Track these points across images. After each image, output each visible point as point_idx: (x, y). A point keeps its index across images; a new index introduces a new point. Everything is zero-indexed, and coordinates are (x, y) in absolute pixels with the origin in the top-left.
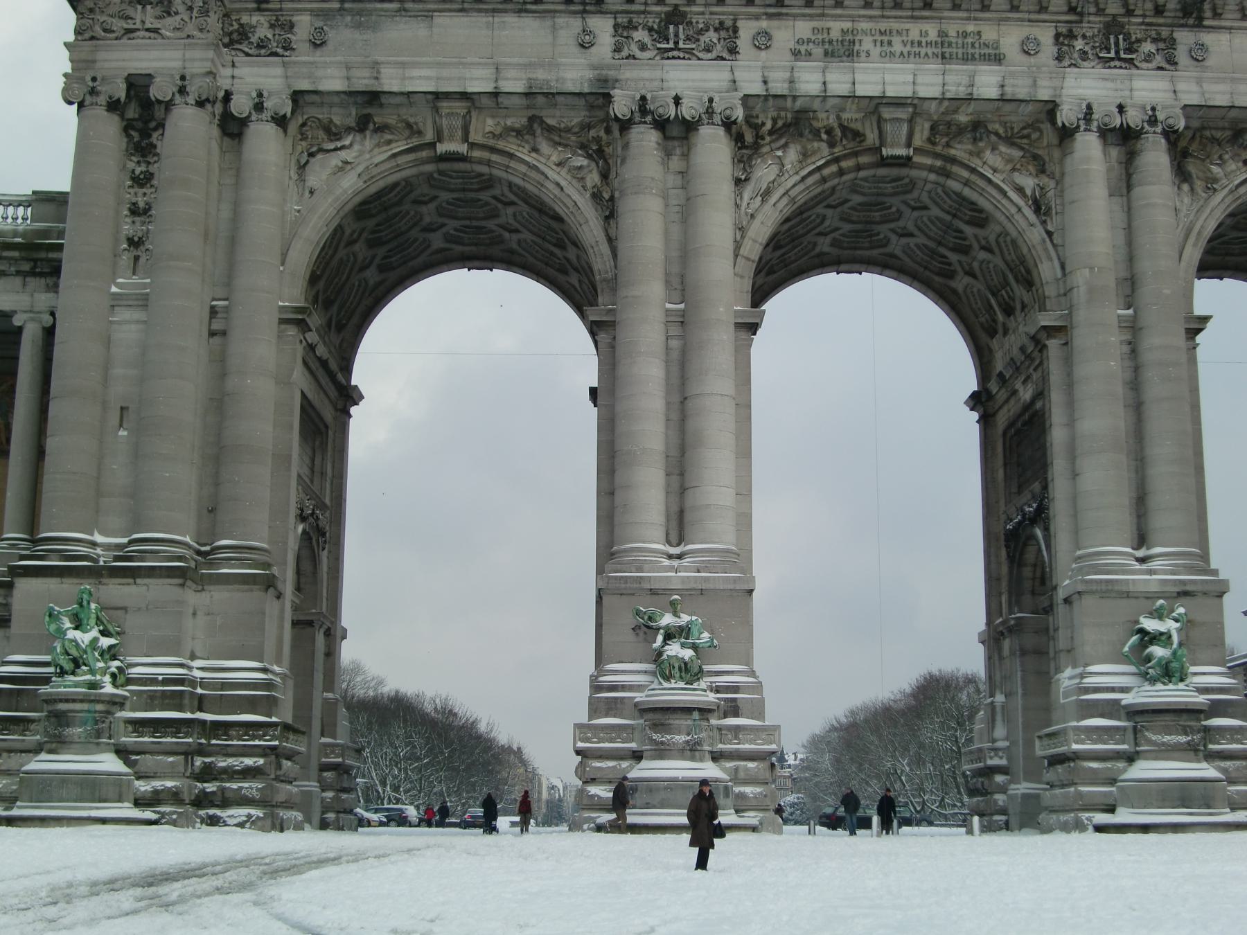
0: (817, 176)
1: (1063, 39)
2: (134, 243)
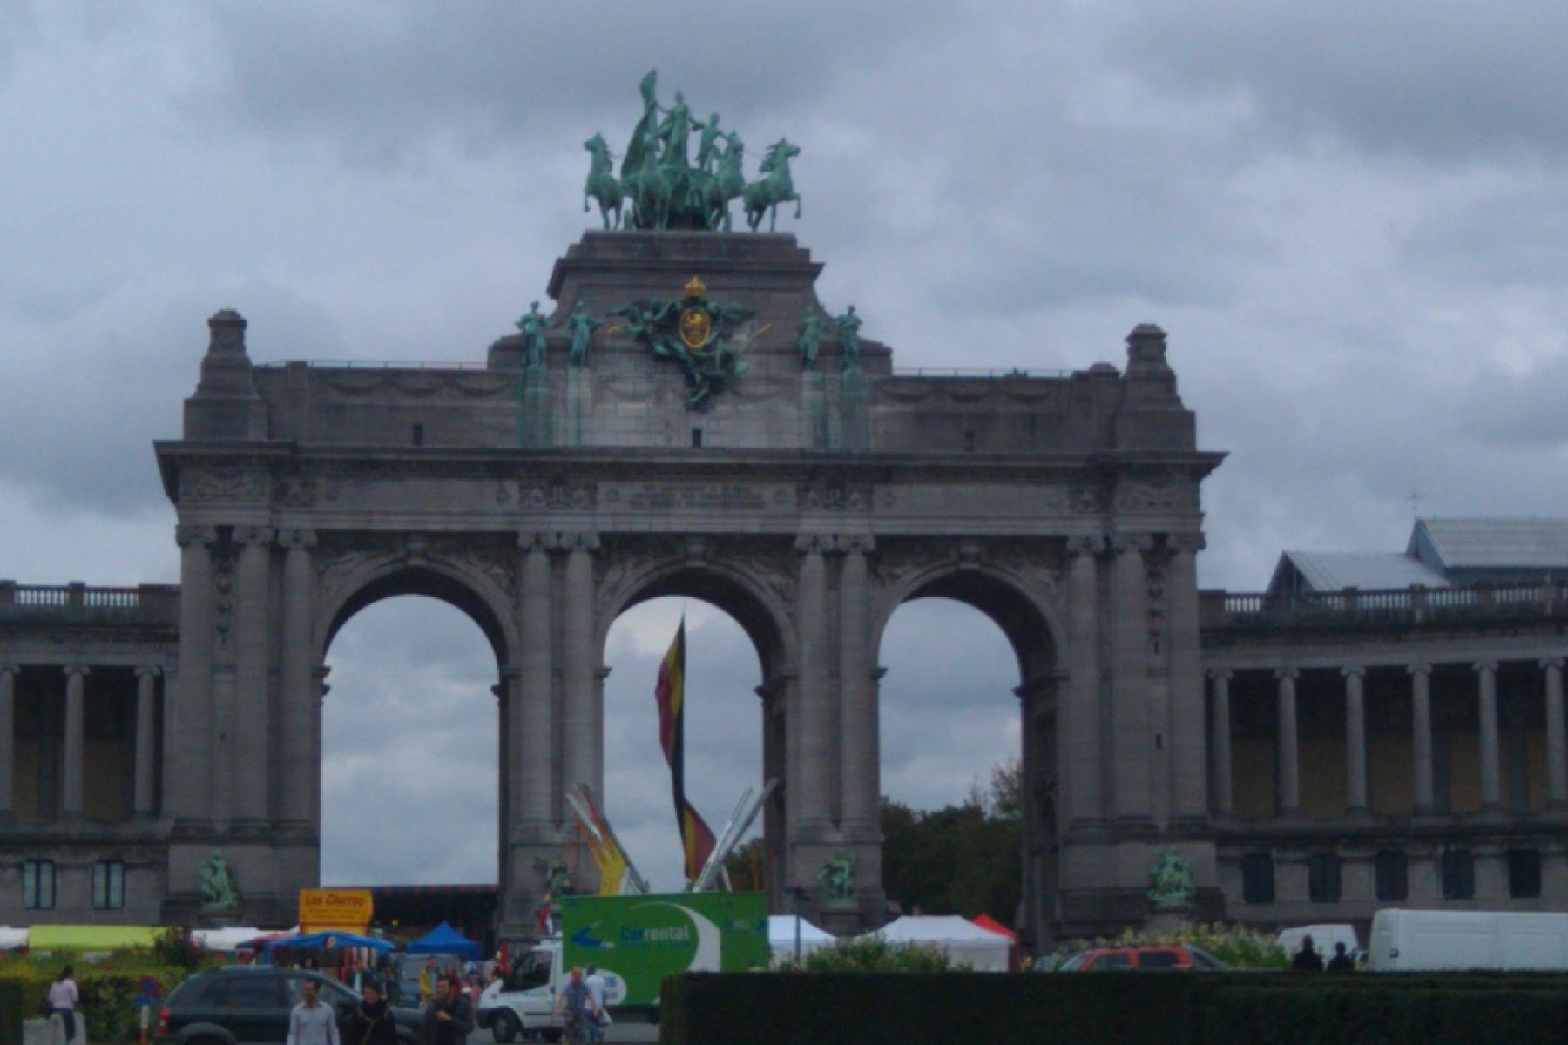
0: (645, 579)
1: (802, 492)
2: (223, 630)
